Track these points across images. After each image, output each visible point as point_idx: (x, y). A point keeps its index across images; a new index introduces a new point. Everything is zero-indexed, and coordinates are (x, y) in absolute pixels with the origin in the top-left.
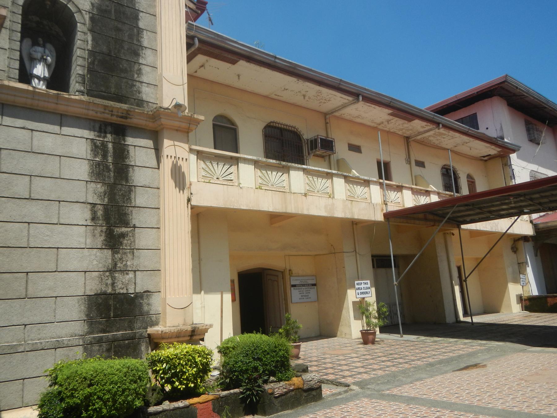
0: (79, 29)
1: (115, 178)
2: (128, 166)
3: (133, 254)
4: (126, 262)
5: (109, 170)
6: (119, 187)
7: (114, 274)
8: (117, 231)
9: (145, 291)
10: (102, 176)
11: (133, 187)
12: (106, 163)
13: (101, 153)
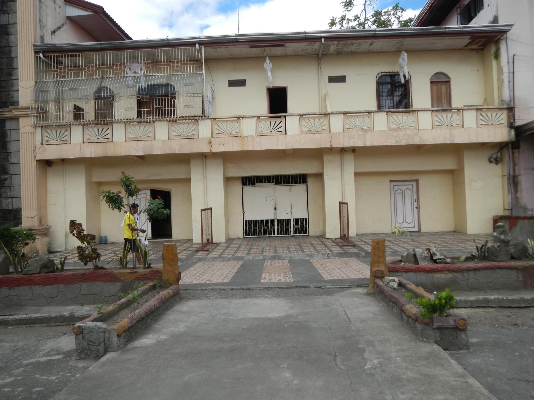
2: (7, 142)
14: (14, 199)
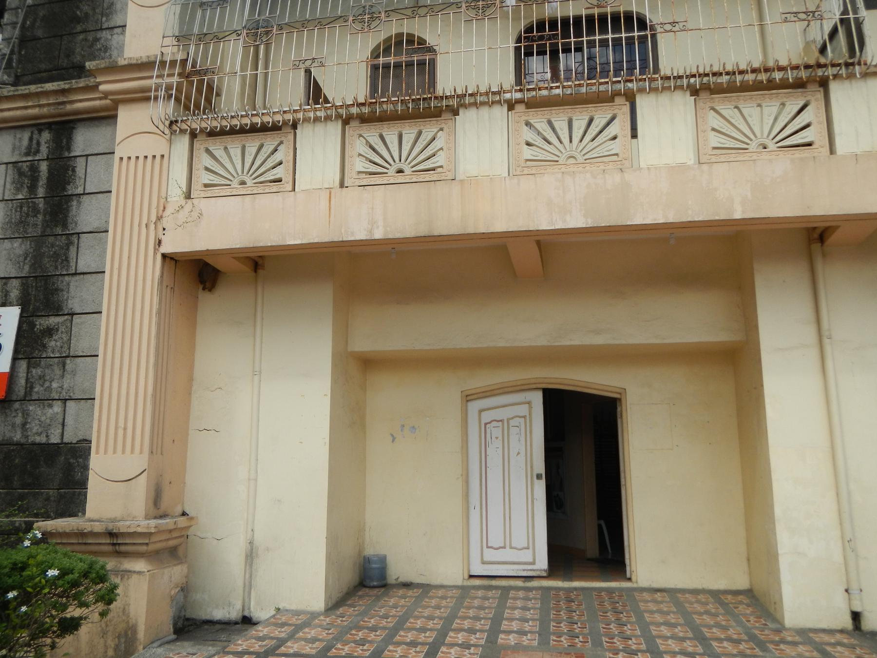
1: (46, 224)
3: (64, 366)
4: (51, 382)
5: (38, 212)
6: (50, 241)
7: (26, 406)
8: (40, 324)
9: (80, 441)
10: (24, 226)
11: (75, 236)
12: (34, 200)
13: (28, 183)
14: (69, 403)
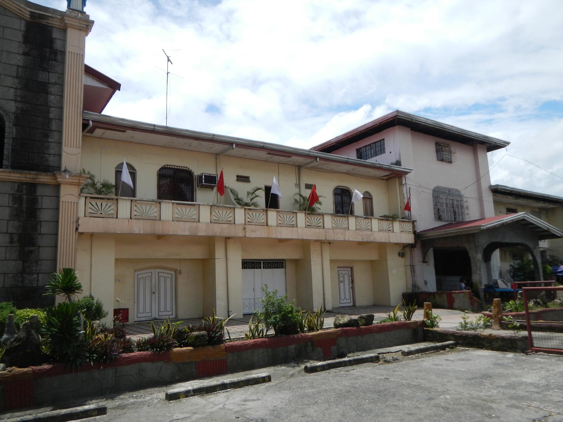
0: (7, 126)
